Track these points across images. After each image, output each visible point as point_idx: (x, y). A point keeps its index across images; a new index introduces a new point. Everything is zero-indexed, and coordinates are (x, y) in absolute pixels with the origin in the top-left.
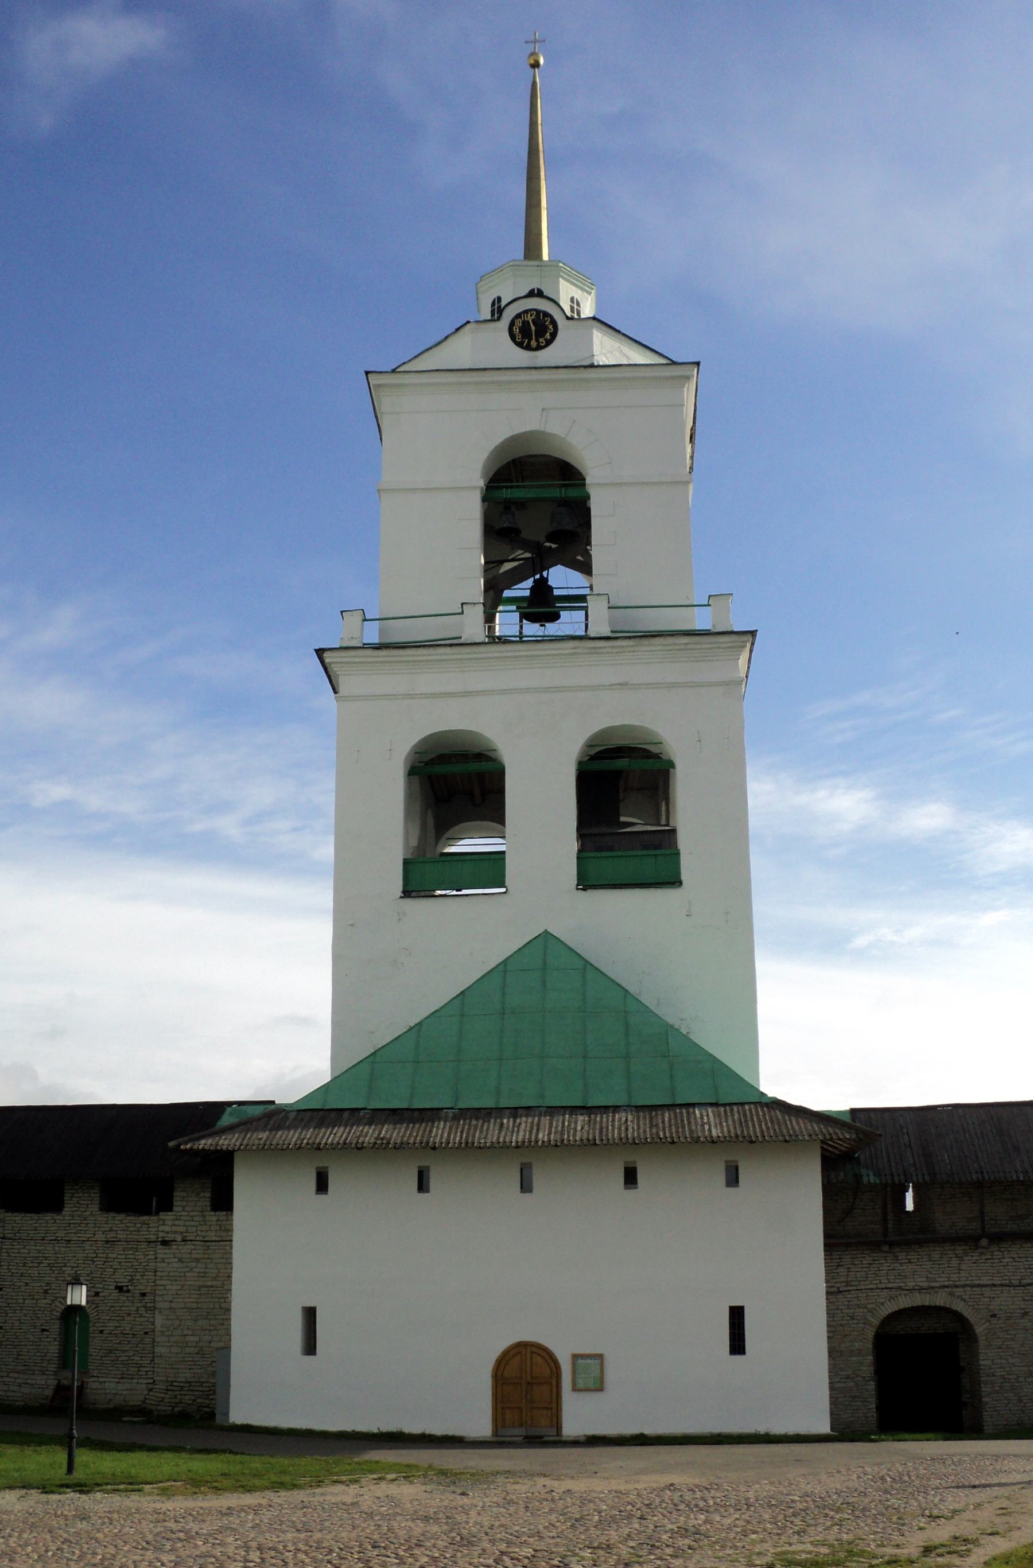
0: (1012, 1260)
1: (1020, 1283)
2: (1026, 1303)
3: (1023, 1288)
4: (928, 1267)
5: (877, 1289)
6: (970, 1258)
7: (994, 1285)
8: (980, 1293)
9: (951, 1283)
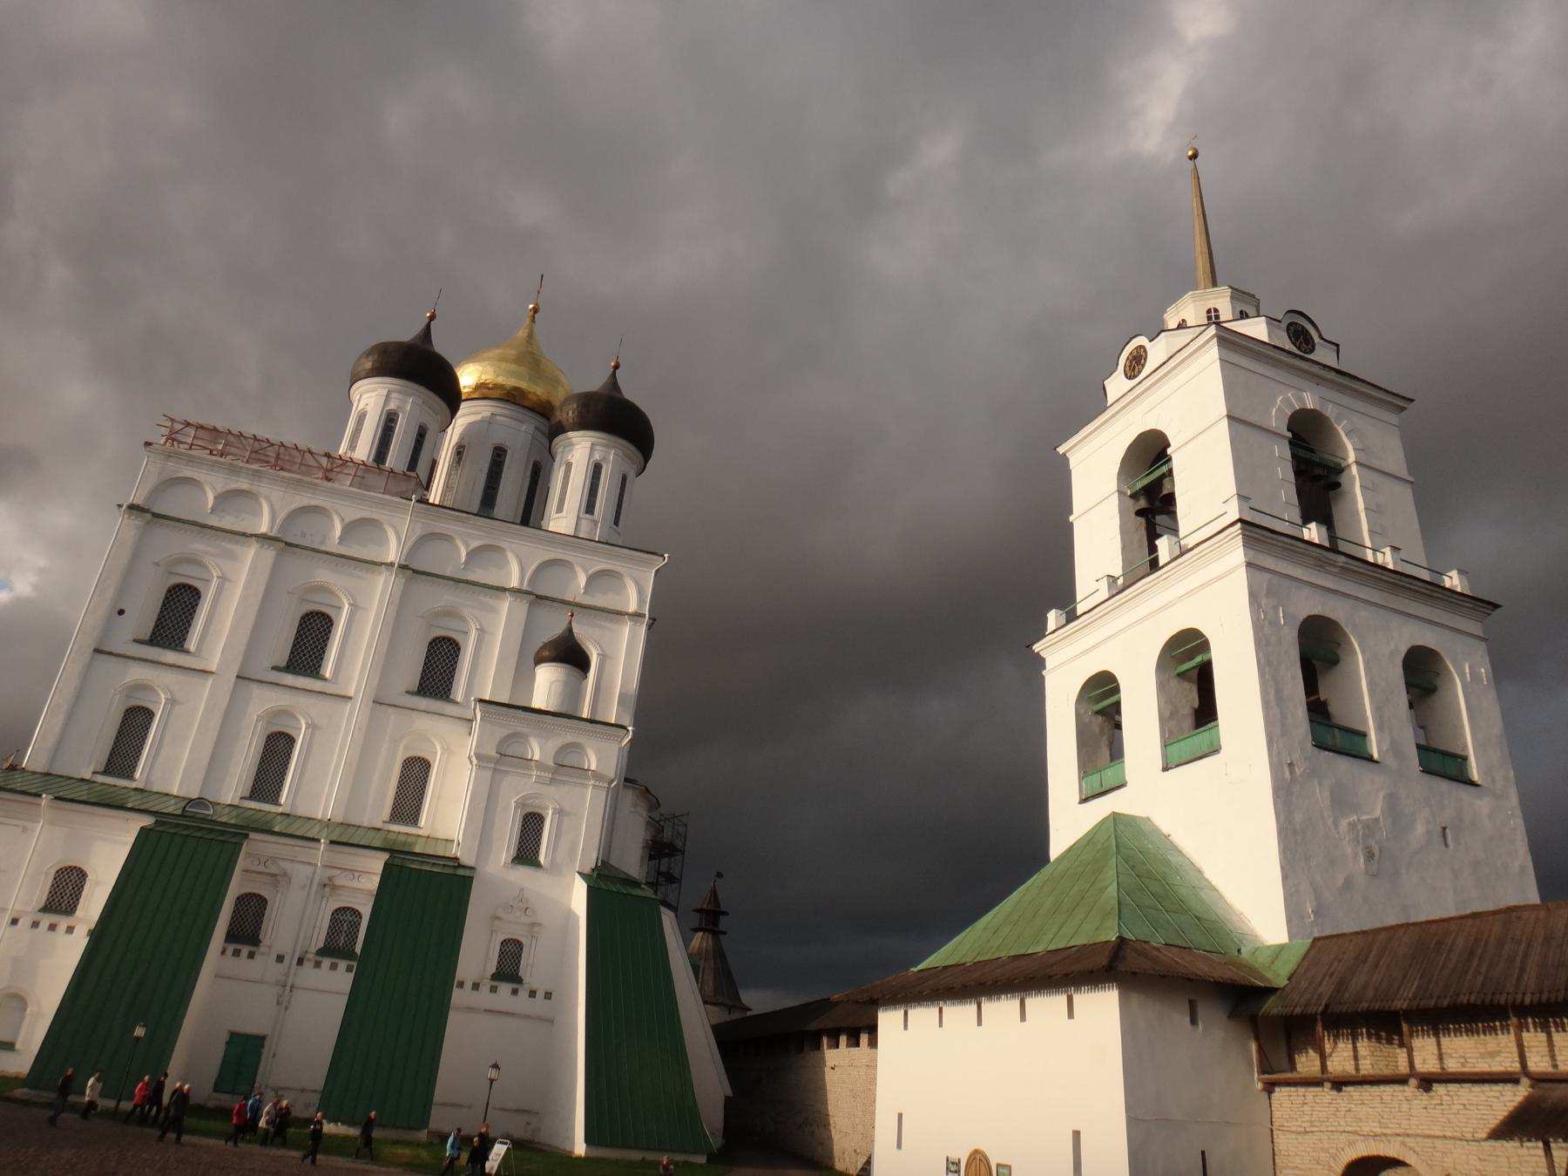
0: (1462, 1107)
1: (1474, 1137)
2: (1483, 1163)
3: (1477, 1144)
4: (1380, 1110)
5: (1337, 1132)
6: (1419, 1102)
7: (1445, 1137)
8: (1432, 1145)
9: (1403, 1131)
